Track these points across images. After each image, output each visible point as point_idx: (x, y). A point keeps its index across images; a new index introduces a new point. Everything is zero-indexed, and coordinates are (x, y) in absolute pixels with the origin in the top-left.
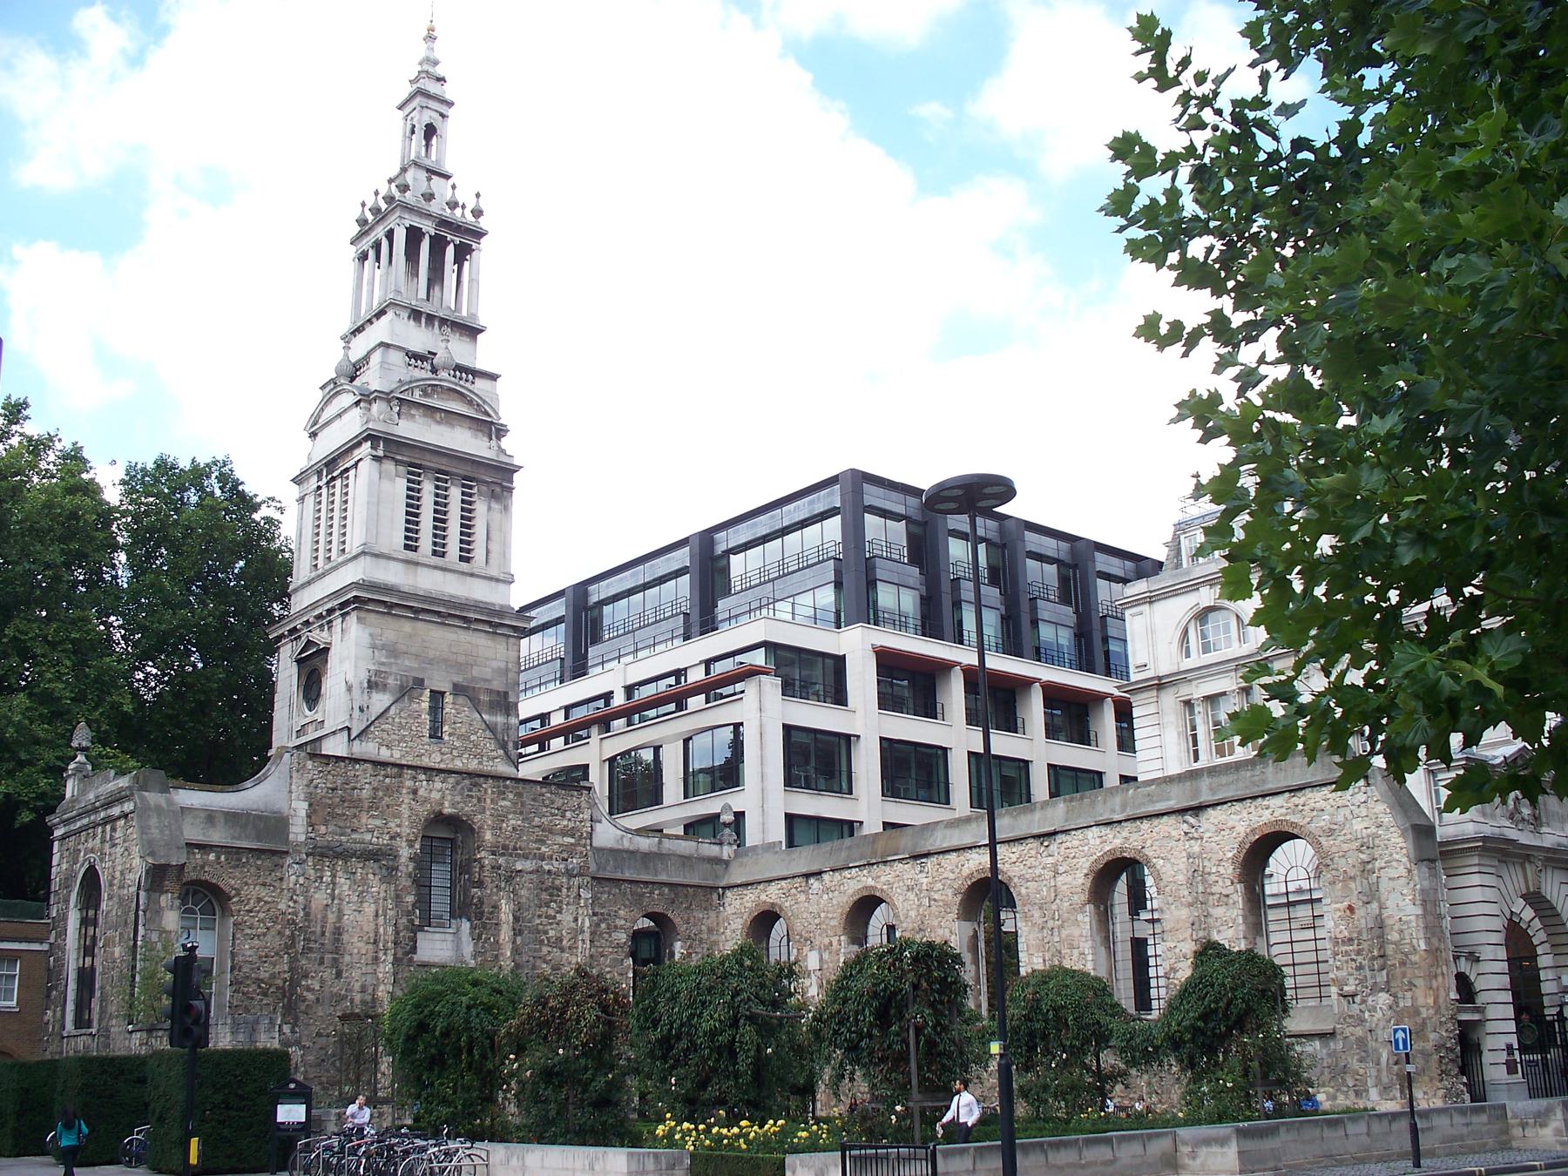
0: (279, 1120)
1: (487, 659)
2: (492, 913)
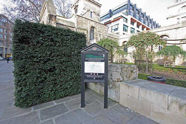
0: (86, 71)
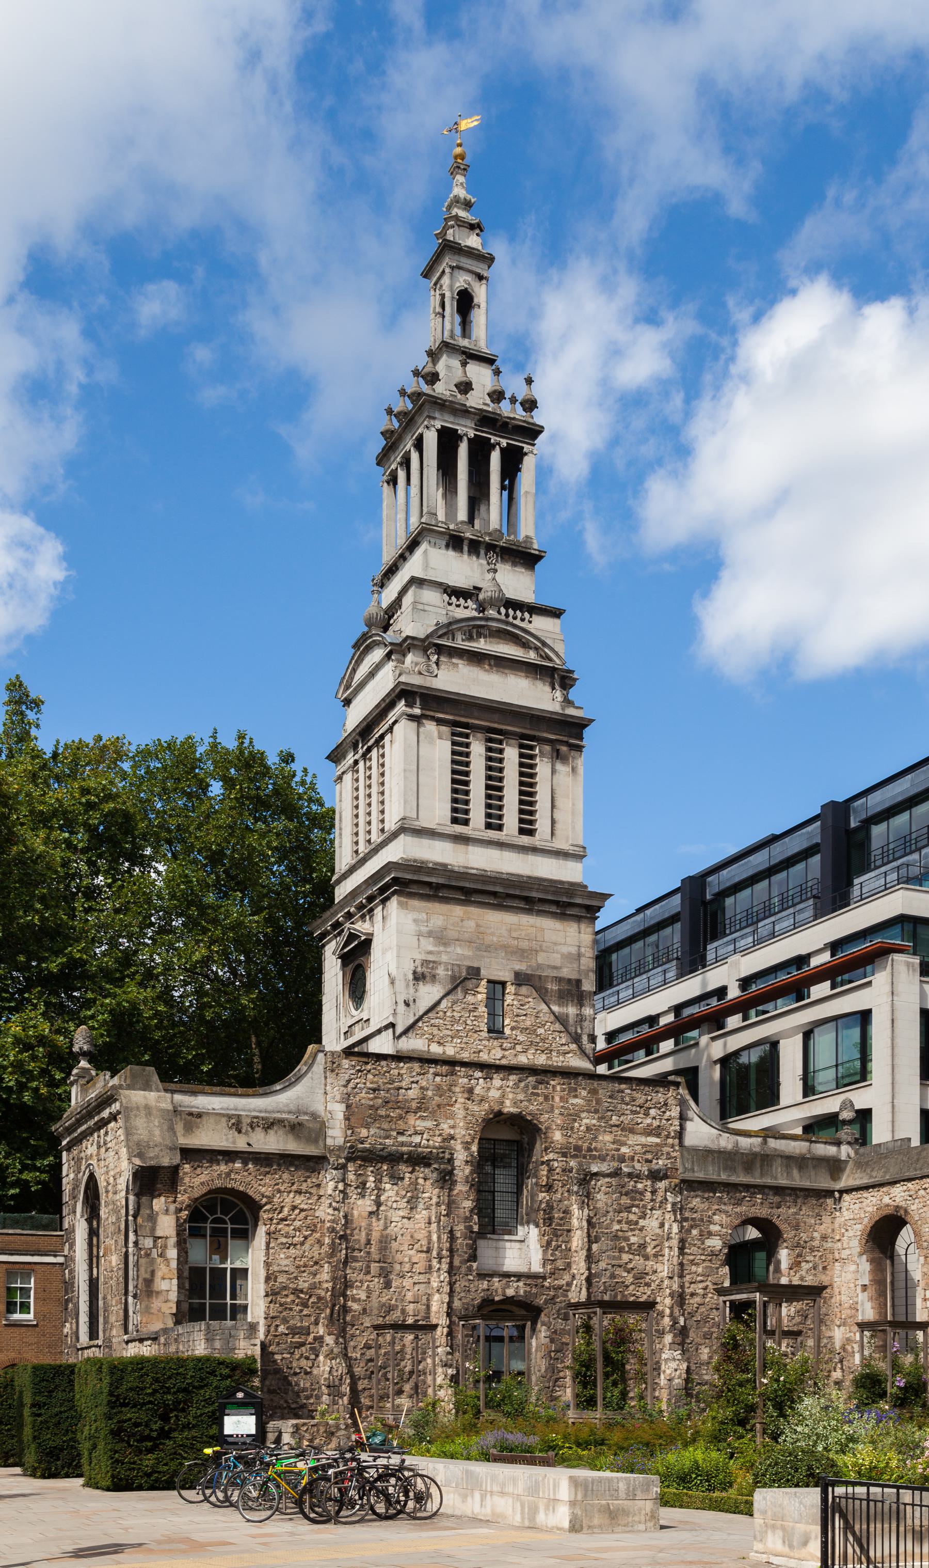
1: (555, 944)
2: (561, 1219)
